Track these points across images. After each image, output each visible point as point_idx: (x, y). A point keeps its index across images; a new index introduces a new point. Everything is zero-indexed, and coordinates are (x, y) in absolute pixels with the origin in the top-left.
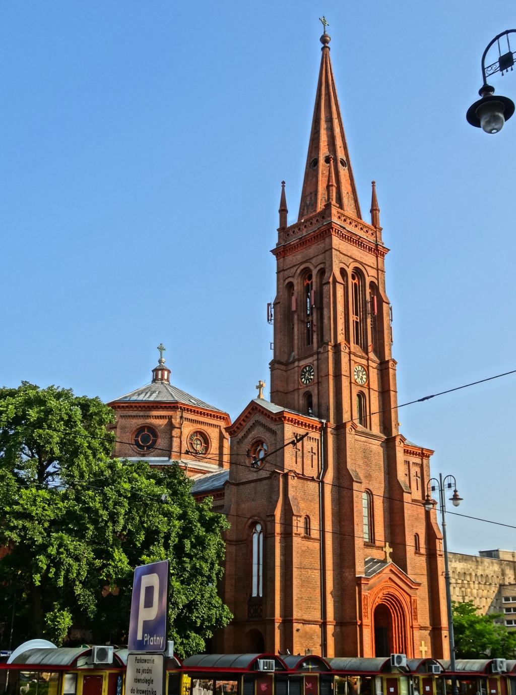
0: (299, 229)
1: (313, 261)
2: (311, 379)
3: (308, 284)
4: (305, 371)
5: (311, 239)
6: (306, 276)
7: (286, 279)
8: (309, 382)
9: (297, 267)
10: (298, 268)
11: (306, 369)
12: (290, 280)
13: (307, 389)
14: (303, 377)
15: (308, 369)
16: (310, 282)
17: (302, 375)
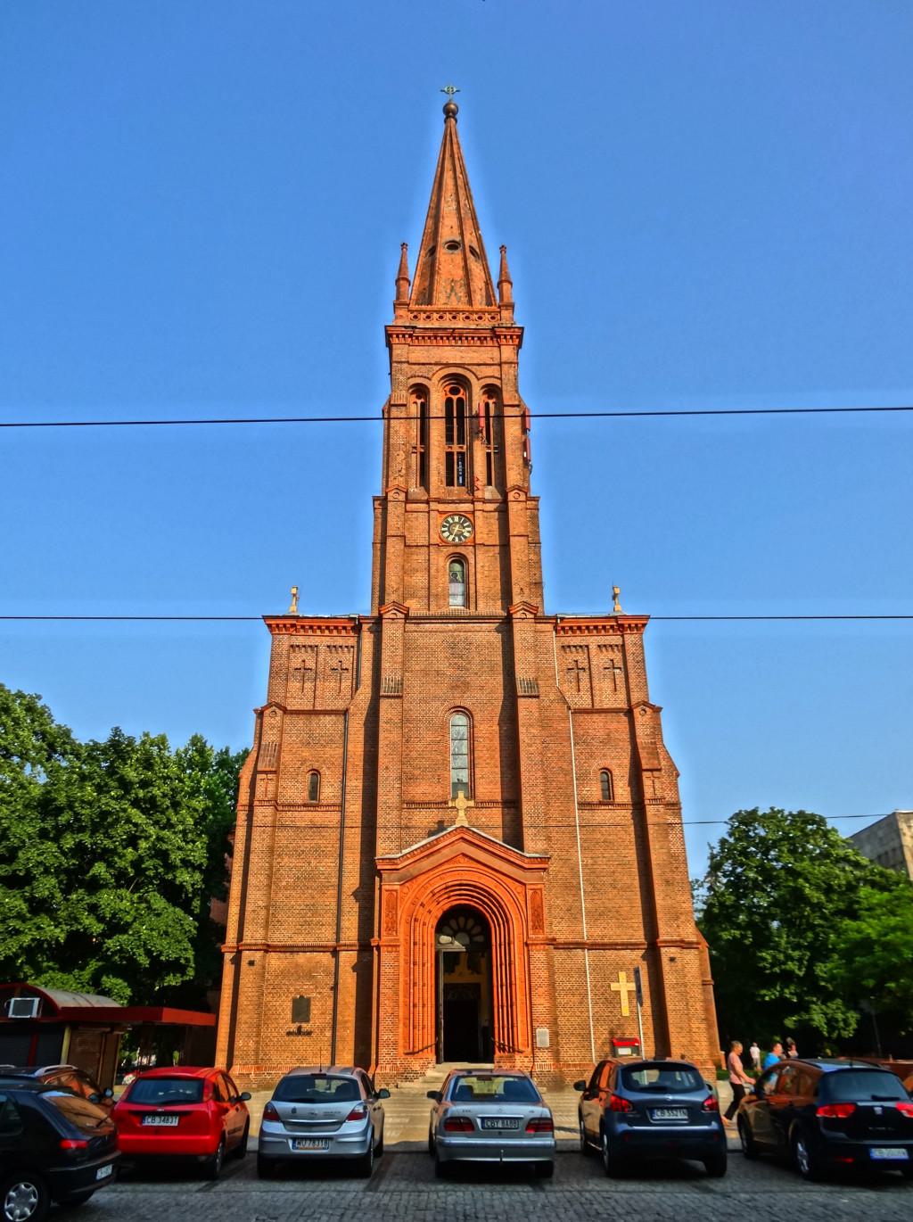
0: (441, 317)
1: (474, 368)
2: (465, 537)
3: (449, 401)
4: (451, 522)
5: (473, 338)
6: (448, 389)
7: (412, 377)
8: (460, 540)
9: (440, 367)
10: (440, 369)
11: (453, 519)
12: (425, 382)
13: (458, 550)
14: (446, 529)
15: (456, 519)
16: (455, 398)
17: (444, 526)
